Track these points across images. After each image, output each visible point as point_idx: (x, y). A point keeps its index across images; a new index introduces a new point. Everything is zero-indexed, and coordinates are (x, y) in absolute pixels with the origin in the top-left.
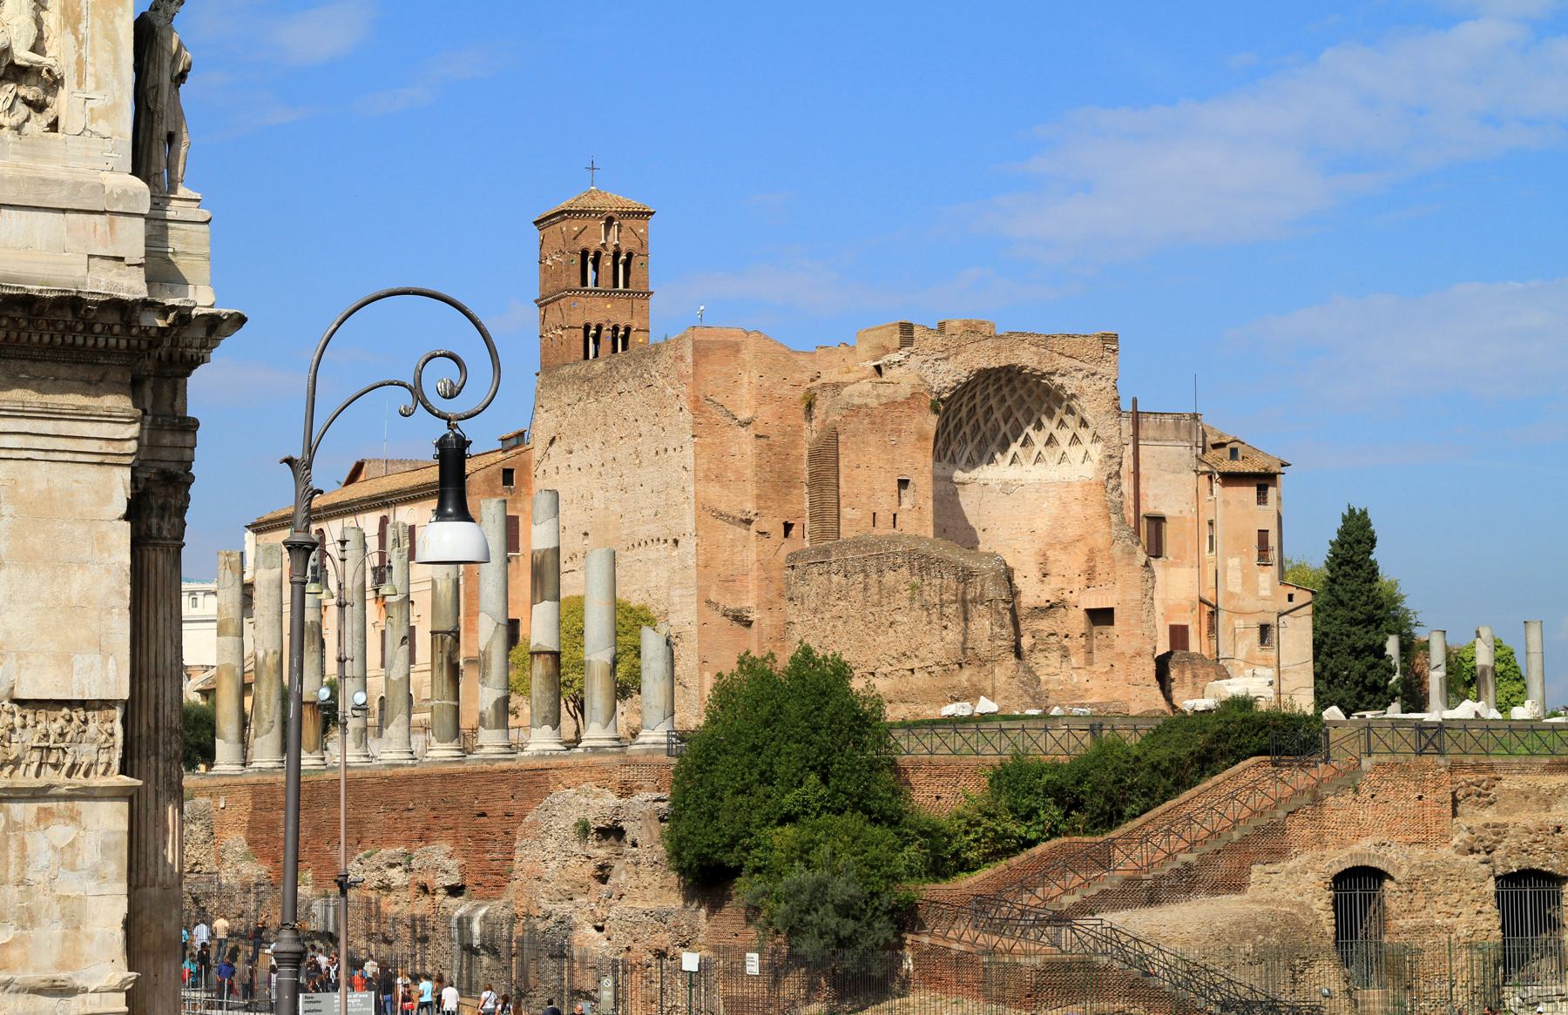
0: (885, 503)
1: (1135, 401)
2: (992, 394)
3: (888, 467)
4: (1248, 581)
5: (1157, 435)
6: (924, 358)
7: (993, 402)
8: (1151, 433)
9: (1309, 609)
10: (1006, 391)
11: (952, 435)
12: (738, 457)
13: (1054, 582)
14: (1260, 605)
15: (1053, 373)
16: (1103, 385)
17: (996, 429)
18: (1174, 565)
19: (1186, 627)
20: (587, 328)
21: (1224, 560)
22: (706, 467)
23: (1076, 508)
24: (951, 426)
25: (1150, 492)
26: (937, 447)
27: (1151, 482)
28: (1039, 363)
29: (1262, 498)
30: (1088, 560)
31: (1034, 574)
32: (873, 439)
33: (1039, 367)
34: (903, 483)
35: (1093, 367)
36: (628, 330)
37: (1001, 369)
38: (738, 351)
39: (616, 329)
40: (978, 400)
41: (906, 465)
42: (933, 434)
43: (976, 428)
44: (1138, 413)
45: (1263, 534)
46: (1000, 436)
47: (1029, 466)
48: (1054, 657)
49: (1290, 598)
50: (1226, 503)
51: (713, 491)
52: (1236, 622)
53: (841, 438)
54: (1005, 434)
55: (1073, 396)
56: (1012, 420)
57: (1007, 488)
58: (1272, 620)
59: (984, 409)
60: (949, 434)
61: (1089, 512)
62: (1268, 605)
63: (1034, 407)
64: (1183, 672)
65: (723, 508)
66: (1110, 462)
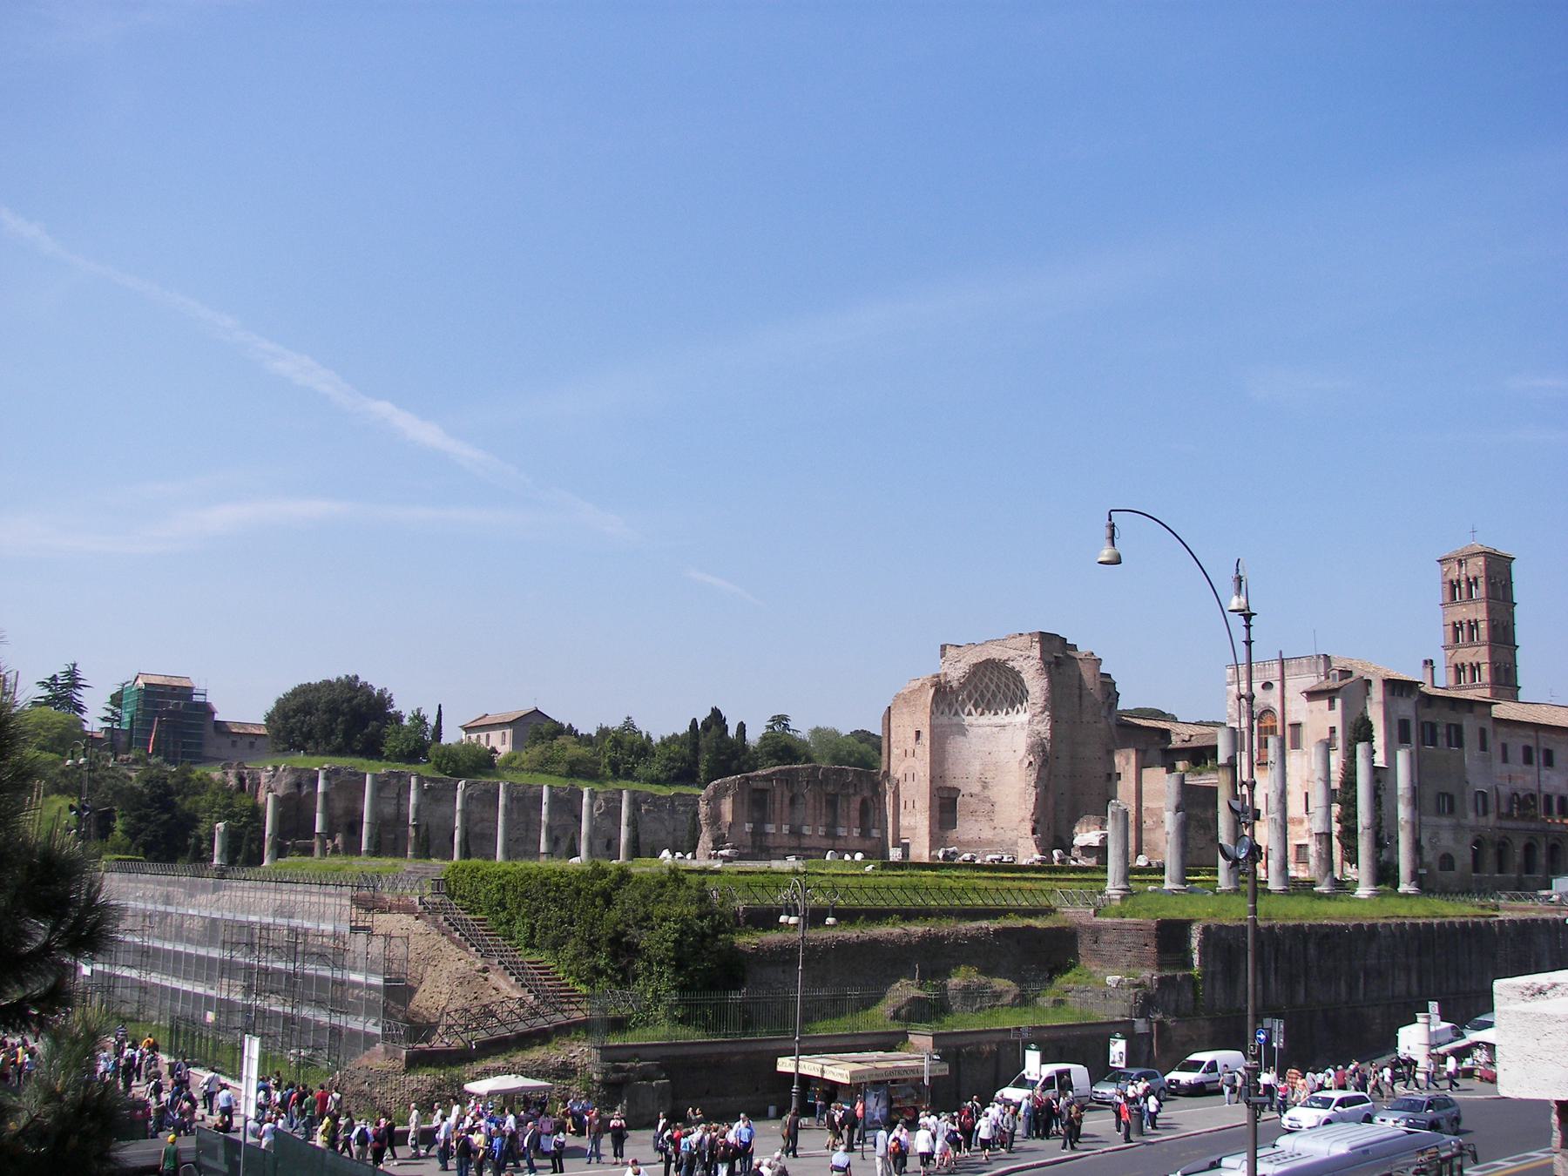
6: (949, 662)
7: (1004, 679)
17: (1015, 694)
20: (1454, 624)
24: (989, 696)
27: (1293, 702)
29: (1331, 707)
32: (905, 710)
33: (1001, 658)
35: (1028, 653)
36: (1476, 621)
39: (1469, 622)
40: (995, 679)
42: (929, 705)
43: (1005, 695)
44: (1283, 659)
53: (892, 712)
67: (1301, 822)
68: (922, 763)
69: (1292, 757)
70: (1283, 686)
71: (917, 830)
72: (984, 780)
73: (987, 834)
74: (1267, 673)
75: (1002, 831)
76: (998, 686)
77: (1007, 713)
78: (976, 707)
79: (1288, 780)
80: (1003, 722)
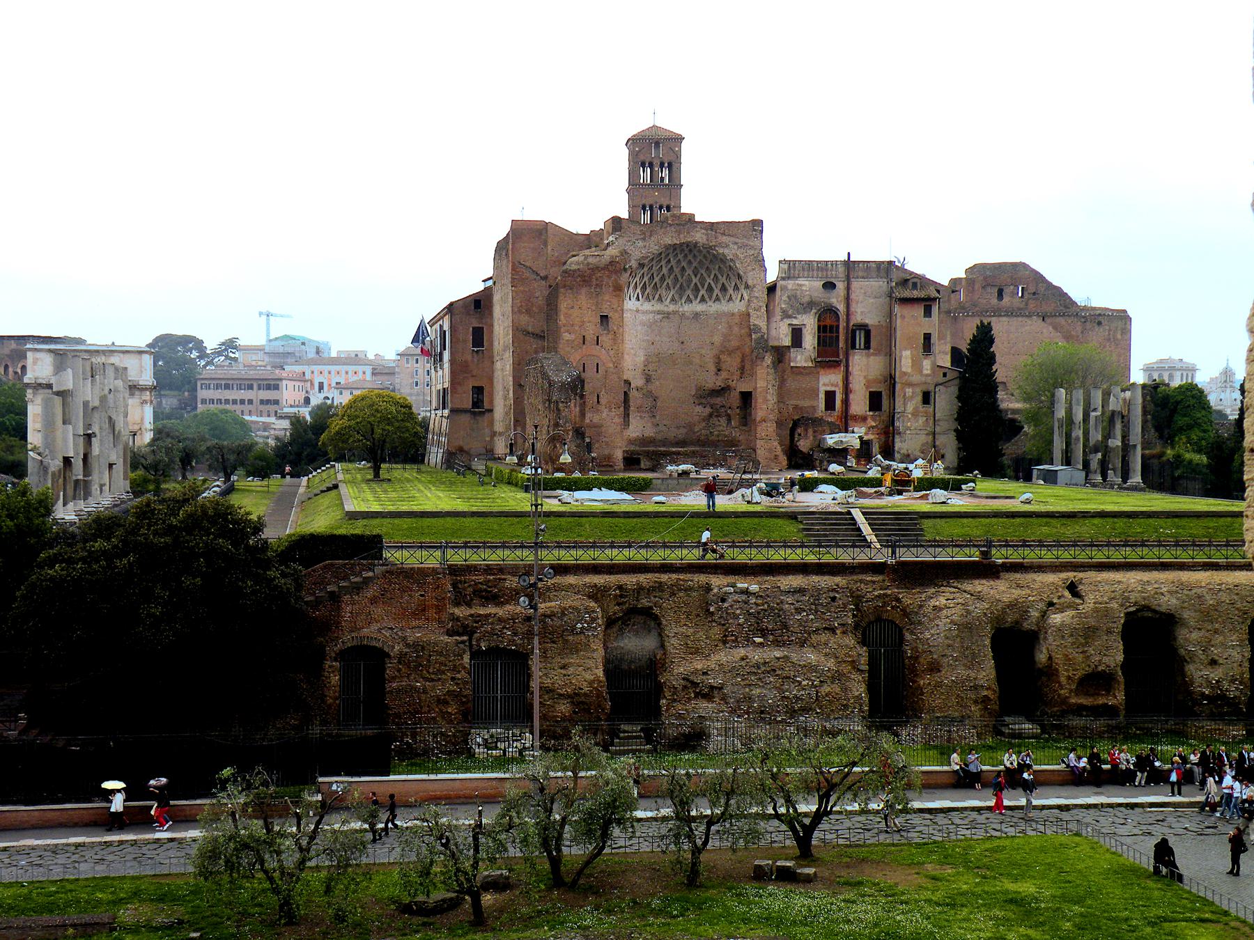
0: (592, 329)
1: (849, 253)
2: (682, 259)
3: (594, 308)
4: (917, 365)
5: (865, 274)
7: (684, 264)
8: (860, 274)
9: (957, 382)
10: (690, 257)
11: (658, 286)
12: (540, 298)
13: (724, 375)
14: (923, 379)
15: (715, 246)
16: (753, 252)
17: (690, 281)
18: (875, 355)
19: (881, 392)
21: (901, 352)
22: (519, 305)
23: (736, 329)
24: (657, 279)
25: (859, 311)
26: (646, 293)
28: (707, 240)
29: (928, 313)
30: (743, 361)
31: (712, 368)
34: (604, 318)
37: (682, 244)
38: (541, 234)
40: (673, 262)
41: (606, 306)
45: (927, 337)
46: (692, 285)
47: (710, 303)
48: (723, 421)
49: (945, 375)
50: (903, 317)
51: (524, 319)
52: (907, 390)
54: (696, 284)
55: (732, 260)
56: (699, 276)
57: (696, 315)
58: (931, 388)
59: (679, 269)
60: (656, 283)
61: (743, 331)
62: (929, 380)
63: (711, 266)
64: (806, 430)
65: (530, 329)
66: (755, 301)
67: (864, 419)
68: (612, 353)
69: (856, 357)
70: (848, 288)
71: (603, 429)
72: (646, 371)
73: (650, 432)
74: (829, 273)
75: (664, 428)
76: (671, 269)
77: (673, 300)
78: (644, 288)
79: (851, 378)
80: (666, 309)
